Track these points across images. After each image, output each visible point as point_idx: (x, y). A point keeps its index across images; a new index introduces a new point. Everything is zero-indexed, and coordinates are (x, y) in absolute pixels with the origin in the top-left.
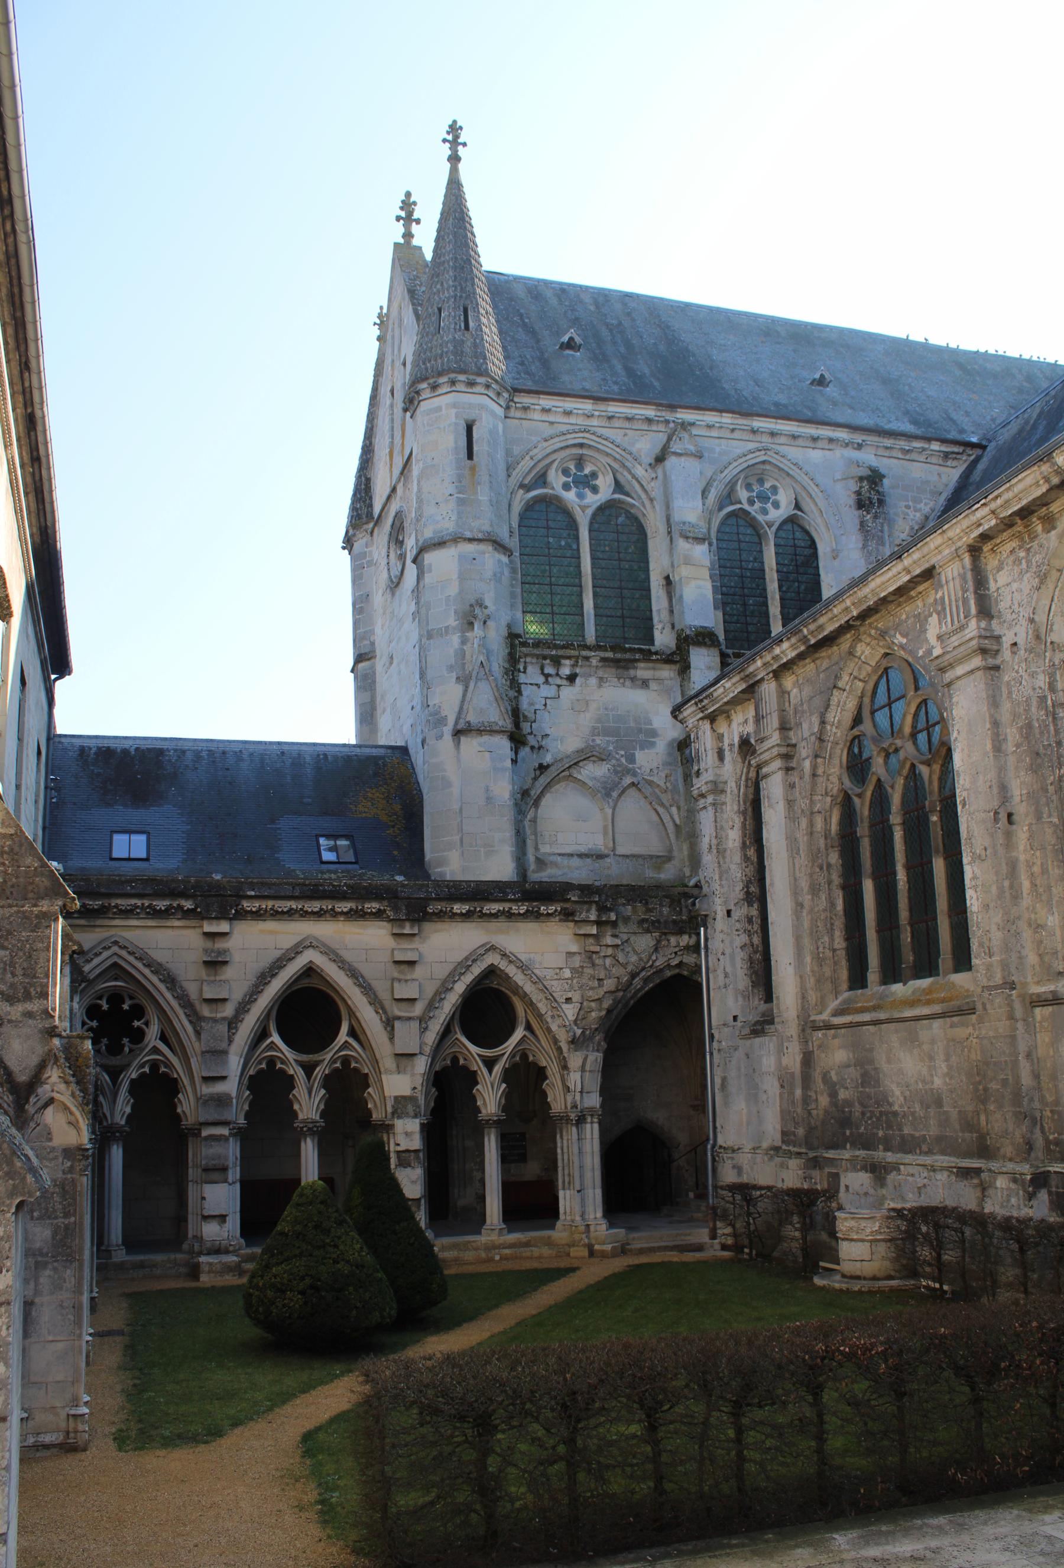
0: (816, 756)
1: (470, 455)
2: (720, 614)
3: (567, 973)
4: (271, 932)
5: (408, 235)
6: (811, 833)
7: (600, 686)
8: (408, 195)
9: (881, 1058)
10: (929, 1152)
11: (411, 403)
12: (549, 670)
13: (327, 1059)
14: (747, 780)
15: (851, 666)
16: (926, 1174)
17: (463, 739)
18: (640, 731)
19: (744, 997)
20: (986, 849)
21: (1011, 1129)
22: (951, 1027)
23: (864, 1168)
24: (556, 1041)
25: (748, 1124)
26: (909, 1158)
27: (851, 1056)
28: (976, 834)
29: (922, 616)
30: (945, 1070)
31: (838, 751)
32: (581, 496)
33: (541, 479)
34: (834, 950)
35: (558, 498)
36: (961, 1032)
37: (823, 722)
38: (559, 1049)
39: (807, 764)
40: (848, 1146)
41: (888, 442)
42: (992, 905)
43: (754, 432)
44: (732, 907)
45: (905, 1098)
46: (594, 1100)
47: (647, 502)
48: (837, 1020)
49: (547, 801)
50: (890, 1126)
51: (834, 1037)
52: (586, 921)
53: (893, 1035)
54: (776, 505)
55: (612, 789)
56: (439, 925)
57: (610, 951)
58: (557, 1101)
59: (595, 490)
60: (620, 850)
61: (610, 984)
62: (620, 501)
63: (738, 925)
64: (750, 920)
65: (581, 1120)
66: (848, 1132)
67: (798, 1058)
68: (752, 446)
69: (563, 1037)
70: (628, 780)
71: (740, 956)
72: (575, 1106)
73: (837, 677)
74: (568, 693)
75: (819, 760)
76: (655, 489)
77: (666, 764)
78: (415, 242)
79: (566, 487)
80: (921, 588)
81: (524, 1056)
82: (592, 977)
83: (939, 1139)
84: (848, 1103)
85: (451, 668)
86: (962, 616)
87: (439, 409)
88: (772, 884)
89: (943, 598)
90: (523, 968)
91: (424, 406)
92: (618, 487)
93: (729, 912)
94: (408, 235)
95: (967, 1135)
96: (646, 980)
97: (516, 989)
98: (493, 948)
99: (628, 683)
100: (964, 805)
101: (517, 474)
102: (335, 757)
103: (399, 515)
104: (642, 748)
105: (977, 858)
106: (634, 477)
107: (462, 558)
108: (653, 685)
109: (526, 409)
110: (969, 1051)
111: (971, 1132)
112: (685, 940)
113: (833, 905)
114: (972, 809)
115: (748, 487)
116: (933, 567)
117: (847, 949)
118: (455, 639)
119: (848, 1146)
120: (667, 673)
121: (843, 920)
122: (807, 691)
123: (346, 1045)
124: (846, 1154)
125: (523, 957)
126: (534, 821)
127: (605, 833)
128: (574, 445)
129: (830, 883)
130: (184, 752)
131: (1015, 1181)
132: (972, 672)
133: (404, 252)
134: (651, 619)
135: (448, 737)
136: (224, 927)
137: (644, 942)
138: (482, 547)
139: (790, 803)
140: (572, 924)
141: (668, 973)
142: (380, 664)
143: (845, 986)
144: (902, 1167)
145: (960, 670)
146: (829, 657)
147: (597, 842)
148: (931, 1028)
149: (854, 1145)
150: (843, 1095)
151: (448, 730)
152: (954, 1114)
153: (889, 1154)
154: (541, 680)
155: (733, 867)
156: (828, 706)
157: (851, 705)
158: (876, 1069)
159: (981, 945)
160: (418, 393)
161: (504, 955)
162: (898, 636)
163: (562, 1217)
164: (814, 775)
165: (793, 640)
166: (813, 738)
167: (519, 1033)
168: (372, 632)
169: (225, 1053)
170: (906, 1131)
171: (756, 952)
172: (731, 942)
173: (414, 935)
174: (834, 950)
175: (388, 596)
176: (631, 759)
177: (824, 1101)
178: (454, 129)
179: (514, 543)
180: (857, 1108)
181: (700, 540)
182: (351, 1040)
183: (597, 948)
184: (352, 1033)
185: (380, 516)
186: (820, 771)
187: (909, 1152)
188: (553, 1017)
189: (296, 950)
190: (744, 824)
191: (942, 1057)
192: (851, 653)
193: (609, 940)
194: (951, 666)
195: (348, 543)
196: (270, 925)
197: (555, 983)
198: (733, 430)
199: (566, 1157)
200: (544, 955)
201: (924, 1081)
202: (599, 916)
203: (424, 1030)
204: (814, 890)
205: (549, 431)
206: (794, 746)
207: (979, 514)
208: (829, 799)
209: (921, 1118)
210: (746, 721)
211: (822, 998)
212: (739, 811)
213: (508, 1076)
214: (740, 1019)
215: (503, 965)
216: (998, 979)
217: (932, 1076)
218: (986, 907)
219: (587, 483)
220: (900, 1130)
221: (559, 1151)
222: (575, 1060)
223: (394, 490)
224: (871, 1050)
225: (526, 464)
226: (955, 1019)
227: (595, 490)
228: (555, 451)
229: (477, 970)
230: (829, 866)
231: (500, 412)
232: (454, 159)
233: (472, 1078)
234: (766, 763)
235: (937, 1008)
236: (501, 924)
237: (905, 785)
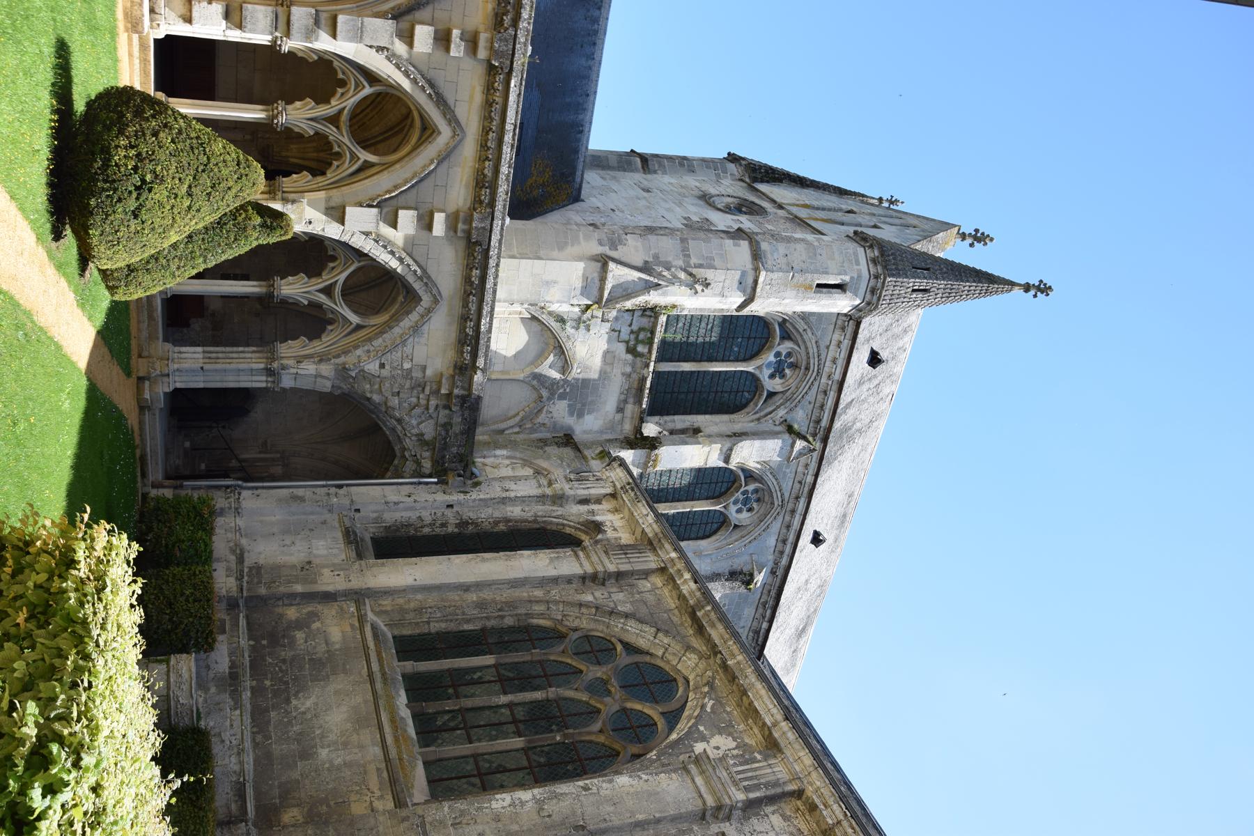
0: (597, 608)
3: (407, 366)
4: (471, 97)
6: (530, 601)
7: (623, 374)
9: (338, 683)
10: (256, 745)
11: (860, 238)
12: (641, 336)
13: (341, 138)
14: (563, 525)
15: (676, 647)
16: (234, 742)
17: (599, 265)
18: (584, 405)
19: (376, 518)
20: (549, 816)
22: (378, 769)
23: (233, 665)
24: (346, 352)
25: (261, 522)
26: (247, 720)
27: (337, 646)
28: (562, 804)
29: (731, 730)
30: (336, 763)
31: (601, 627)
34: (428, 623)
35: (771, 347)
36: (373, 782)
37: (626, 616)
38: (338, 356)
39: (589, 598)
40: (252, 643)
41: (773, 593)
43: (797, 498)
44: (455, 509)
45: (304, 713)
46: (287, 382)
47: (757, 416)
48: (368, 630)
50: (276, 694)
51: (352, 626)
52: (453, 385)
53: (361, 697)
54: (739, 511)
55: (539, 381)
56: (461, 254)
57: (423, 402)
58: (289, 350)
59: (772, 376)
61: (394, 402)
62: (761, 395)
63: (439, 514)
64: (443, 525)
65: (269, 372)
66: (264, 642)
67: (330, 588)
68: (787, 495)
69: (350, 360)
70: (545, 393)
71: (412, 515)
72: (284, 368)
73: (667, 633)
74: (622, 348)
75: (593, 610)
76: (767, 425)
77: (555, 424)
79: (778, 354)
80: (756, 730)
81: (331, 322)
82: (402, 387)
83: (269, 755)
84: (293, 641)
85: (656, 257)
86: (746, 783)
87: (858, 263)
88: (484, 560)
89: (755, 761)
90: (416, 329)
91: (861, 251)
92: (771, 395)
93: (450, 506)
95: (276, 792)
96: (393, 430)
97: (396, 319)
99: (623, 397)
100: (586, 788)
102: (579, 140)
103: (760, 211)
104: (569, 406)
105: (540, 803)
106: (778, 407)
108: (619, 416)
109: (843, 329)
110: (357, 792)
111: (280, 797)
112: (427, 465)
113: (468, 621)
114: (582, 798)
115: (756, 491)
116: (780, 751)
117: (430, 634)
119: (252, 643)
120: (628, 427)
121: (455, 629)
122: (650, 598)
123: (354, 157)
124: (244, 642)
125: (426, 327)
127: (502, 372)
128: (808, 363)
129: (488, 618)
130: (599, 8)
132: (701, 796)
134: (668, 414)
135: (599, 250)
136: (482, 53)
137: (428, 429)
139: (555, 580)
140: (451, 371)
141: (397, 448)
142: (639, 177)
143: (396, 633)
144: (238, 712)
145: (699, 781)
146: (682, 624)
148: (374, 745)
149: (253, 649)
150: (300, 635)
151: (606, 250)
152: (295, 775)
153: (249, 694)
154: (635, 327)
155: (490, 510)
156: (641, 622)
157: (642, 643)
158: (328, 677)
160: (871, 247)
161: (429, 311)
162: (712, 702)
163: (177, 349)
164: (581, 605)
165: (698, 594)
166: (612, 605)
167: (354, 319)
168: (665, 173)
169: (361, 40)
170: (273, 714)
171: (416, 530)
172: (424, 508)
173: (456, 232)
174: (428, 623)
176: (562, 397)
177: (292, 613)
180: (286, 654)
182: (360, 163)
183: (427, 391)
184: (367, 166)
185: (757, 190)
186: (584, 610)
187: (253, 720)
188: (368, 351)
189: (453, 120)
190: (526, 521)
191: (348, 758)
192: (689, 648)
193: (433, 402)
194: (702, 772)
195: (733, 158)
196: (478, 98)
197: (399, 354)
198: (800, 482)
199: (234, 355)
201: (322, 736)
202: (458, 396)
203: (367, 234)
204: (481, 605)
205: (823, 345)
206: (603, 584)
207: (835, 807)
208: (560, 617)
209: (287, 732)
210: (615, 530)
211: (386, 612)
212: (536, 516)
214: (357, 515)
215: (420, 309)
217: (329, 746)
218: (497, 818)
219: (778, 372)
220: (273, 707)
221: (241, 349)
222: (327, 369)
223: (781, 207)
224: (345, 671)
226: (385, 775)
227: (772, 376)
228: (807, 348)
230: (502, 617)
232: (1027, 288)
233: (314, 273)
234: (588, 557)
235: (393, 753)
236: (458, 309)
237: (580, 701)
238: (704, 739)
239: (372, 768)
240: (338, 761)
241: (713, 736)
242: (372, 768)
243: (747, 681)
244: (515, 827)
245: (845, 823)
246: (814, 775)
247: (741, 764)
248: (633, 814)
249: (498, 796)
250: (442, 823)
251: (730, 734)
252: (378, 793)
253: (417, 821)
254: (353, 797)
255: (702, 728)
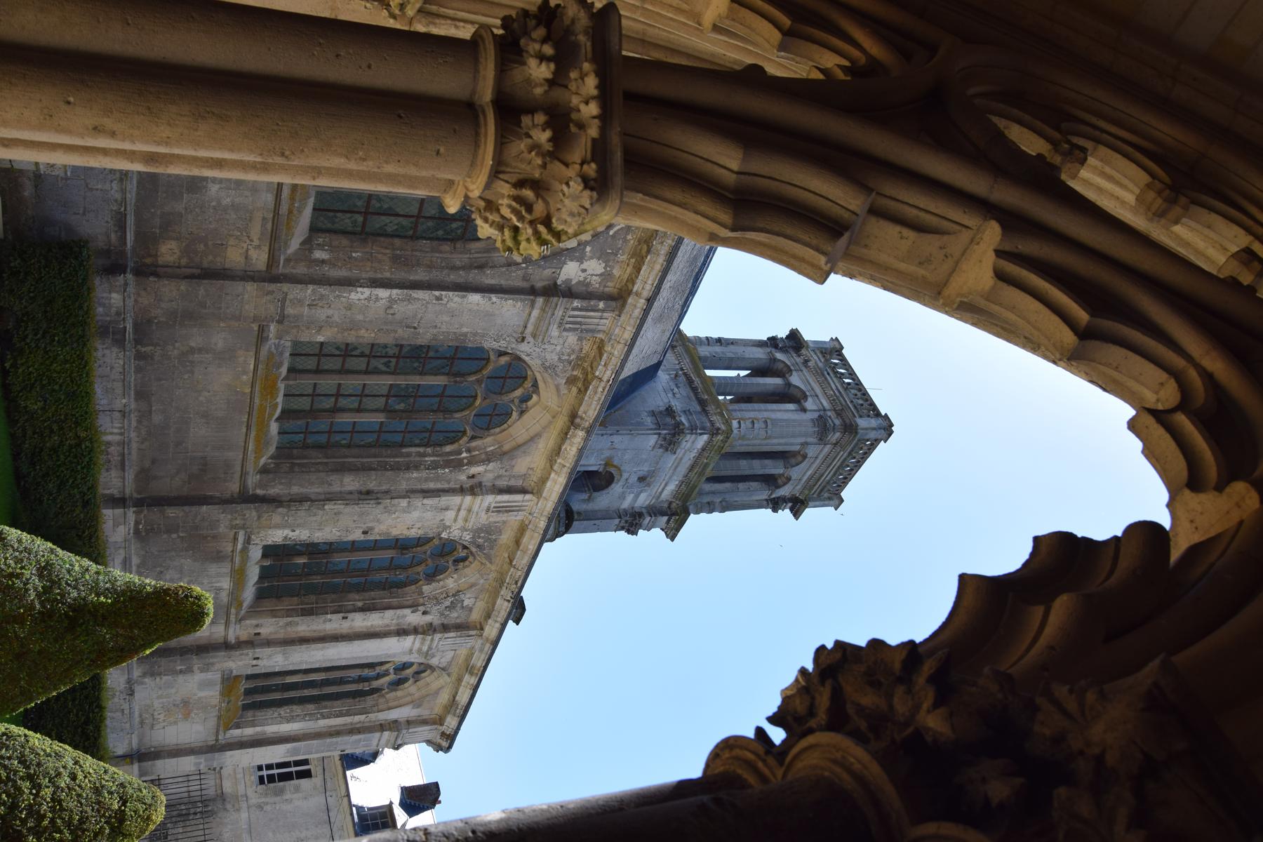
21: (163, 305)
22: (264, 219)
28: (410, 307)
36: (256, 231)
42: (349, 313)
80: (629, 270)
100: (438, 299)
105: (392, 301)
110: (237, 238)
131: (118, 314)
145: (536, 313)
152: (179, 207)
159: (322, 297)
194: (543, 310)
207: (609, 373)
216: (290, 311)
218: (349, 307)
226: (269, 226)
235: (284, 209)
238: (581, 260)
239: (258, 216)
240: (227, 201)
241: (591, 258)
242: (258, 216)
243: (659, 247)
244: (360, 317)
245: (603, 384)
246: (620, 346)
247: (580, 310)
248: (462, 326)
249: (359, 289)
250: (301, 302)
251: (606, 262)
252: (256, 242)
253: (280, 297)
254: (232, 242)
255: (588, 249)
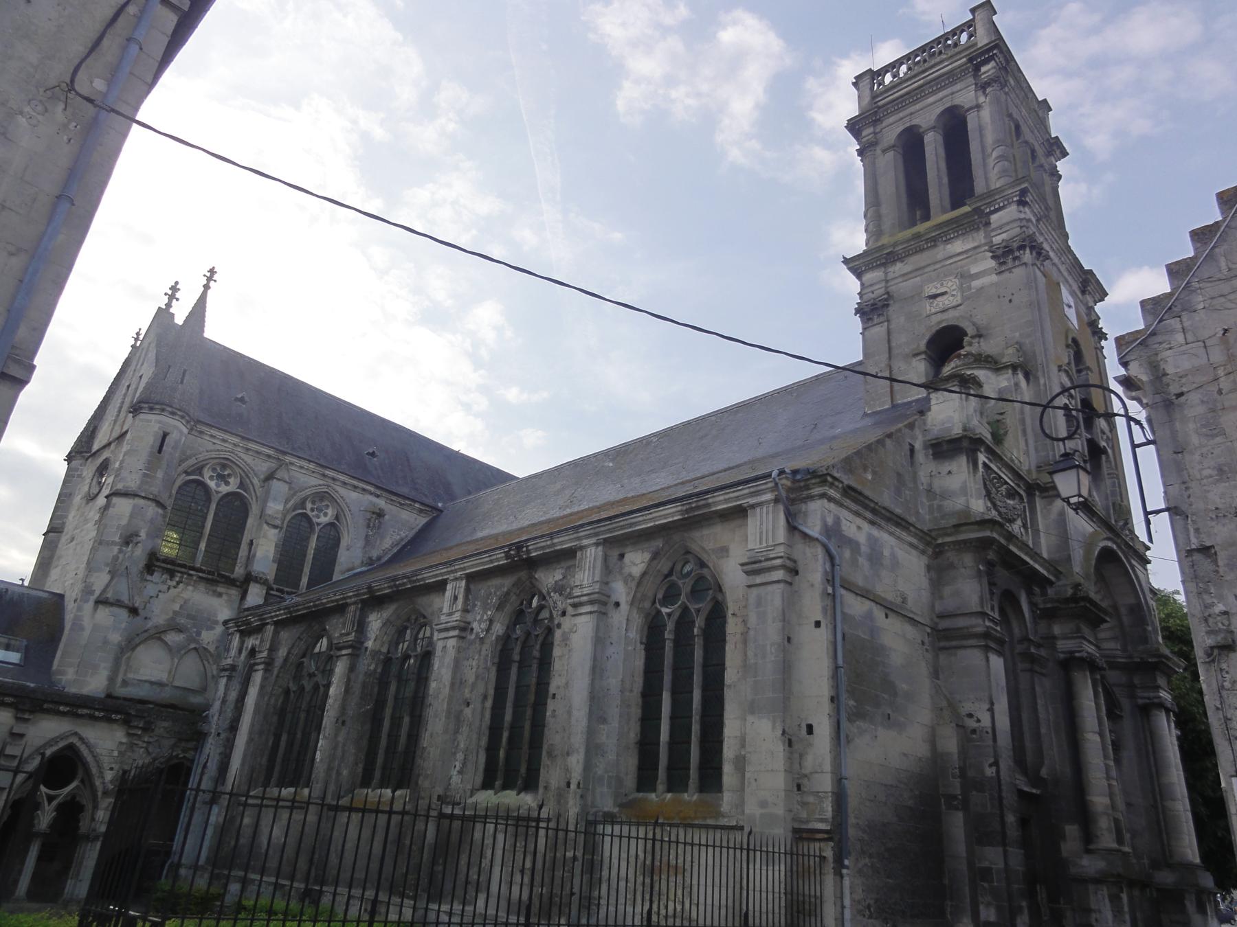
1: (160, 451)
2: (275, 566)
3: (116, 754)
5: (169, 305)
8: (177, 283)
32: (218, 485)
33: (199, 470)
41: (394, 498)
43: (324, 475)
49: (141, 649)
52: (137, 727)
54: (326, 514)
60: (177, 683)
70: (193, 646)
76: (259, 491)
78: (172, 310)
81: (74, 797)
91: (142, 416)
92: (242, 485)
93: (219, 734)
94: (169, 305)
98: (76, 734)
101: (185, 465)
103: (107, 460)
107: (135, 506)
108: (225, 597)
109: (201, 432)
115: (313, 502)
118: (116, 549)
120: (234, 593)
126: (129, 658)
127: (170, 672)
133: (163, 315)
135: (91, 604)
138: (149, 503)
142: (64, 538)
147: (164, 677)
151: (93, 598)
161: (81, 739)
168: (66, 517)
175: (84, 502)
176: (199, 634)
178: (212, 271)
179: (169, 503)
181: (275, 527)
195: (69, 458)
200: (106, 745)
213: (61, 808)
223: (109, 444)
225: (192, 461)
227: (227, 483)
229: (61, 744)
231: (185, 431)
232: (207, 287)
233: (38, 806)
